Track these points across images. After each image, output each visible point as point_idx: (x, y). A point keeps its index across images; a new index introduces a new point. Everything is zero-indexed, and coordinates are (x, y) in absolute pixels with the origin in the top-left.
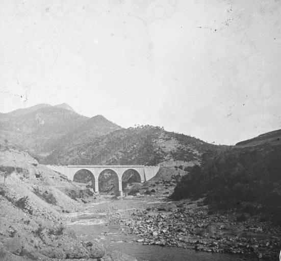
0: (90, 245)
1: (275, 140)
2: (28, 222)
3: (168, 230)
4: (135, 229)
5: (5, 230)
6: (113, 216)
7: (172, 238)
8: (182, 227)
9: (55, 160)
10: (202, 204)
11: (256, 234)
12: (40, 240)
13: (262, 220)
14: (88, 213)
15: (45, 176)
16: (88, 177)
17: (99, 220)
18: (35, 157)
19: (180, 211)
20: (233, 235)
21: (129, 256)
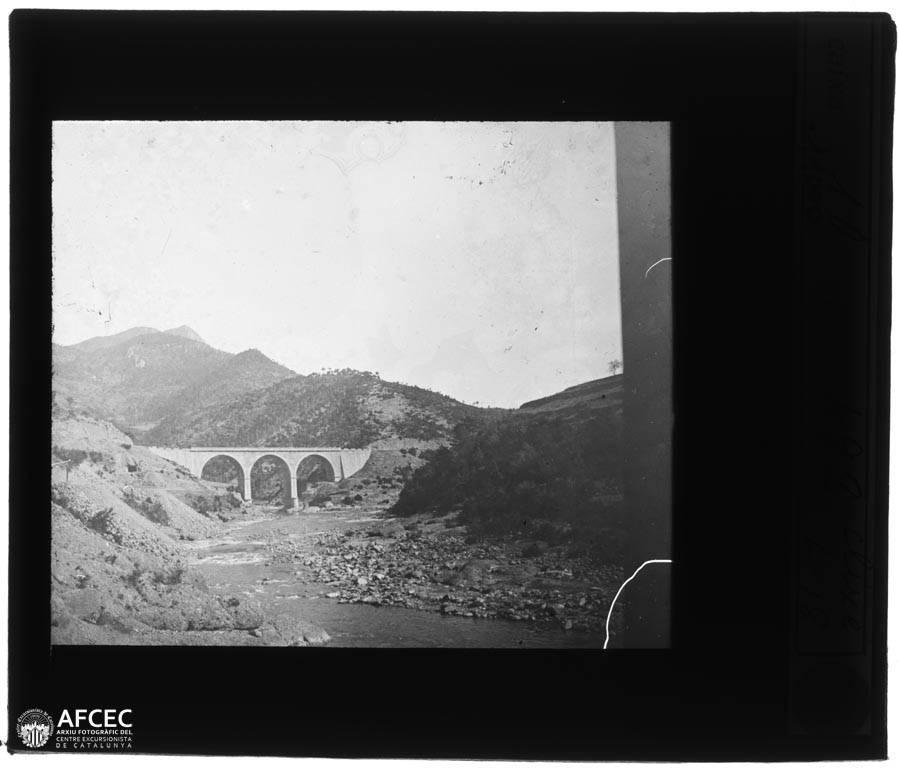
0: (235, 603)
1: (599, 398)
2: (113, 559)
3: (388, 574)
4: (323, 572)
5: (67, 574)
6: (280, 547)
7: (394, 589)
8: (415, 568)
9: (166, 438)
10: (455, 524)
11: (559, 583)
12: (136, 593)
13: (571, 555)
14: (230, 542)
15: (147, 468)
16: (230, 470)
17: (252, 554)
18: (127, 431)
19: (412, 538)
20: (517, 583)
21: (310, 625)
